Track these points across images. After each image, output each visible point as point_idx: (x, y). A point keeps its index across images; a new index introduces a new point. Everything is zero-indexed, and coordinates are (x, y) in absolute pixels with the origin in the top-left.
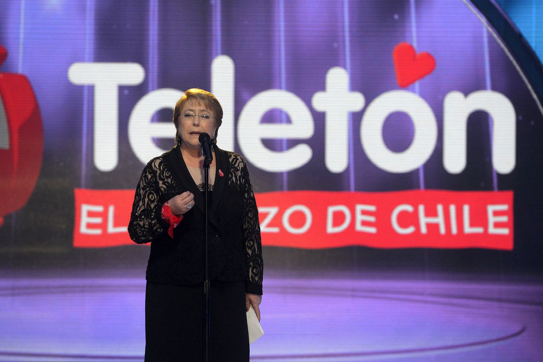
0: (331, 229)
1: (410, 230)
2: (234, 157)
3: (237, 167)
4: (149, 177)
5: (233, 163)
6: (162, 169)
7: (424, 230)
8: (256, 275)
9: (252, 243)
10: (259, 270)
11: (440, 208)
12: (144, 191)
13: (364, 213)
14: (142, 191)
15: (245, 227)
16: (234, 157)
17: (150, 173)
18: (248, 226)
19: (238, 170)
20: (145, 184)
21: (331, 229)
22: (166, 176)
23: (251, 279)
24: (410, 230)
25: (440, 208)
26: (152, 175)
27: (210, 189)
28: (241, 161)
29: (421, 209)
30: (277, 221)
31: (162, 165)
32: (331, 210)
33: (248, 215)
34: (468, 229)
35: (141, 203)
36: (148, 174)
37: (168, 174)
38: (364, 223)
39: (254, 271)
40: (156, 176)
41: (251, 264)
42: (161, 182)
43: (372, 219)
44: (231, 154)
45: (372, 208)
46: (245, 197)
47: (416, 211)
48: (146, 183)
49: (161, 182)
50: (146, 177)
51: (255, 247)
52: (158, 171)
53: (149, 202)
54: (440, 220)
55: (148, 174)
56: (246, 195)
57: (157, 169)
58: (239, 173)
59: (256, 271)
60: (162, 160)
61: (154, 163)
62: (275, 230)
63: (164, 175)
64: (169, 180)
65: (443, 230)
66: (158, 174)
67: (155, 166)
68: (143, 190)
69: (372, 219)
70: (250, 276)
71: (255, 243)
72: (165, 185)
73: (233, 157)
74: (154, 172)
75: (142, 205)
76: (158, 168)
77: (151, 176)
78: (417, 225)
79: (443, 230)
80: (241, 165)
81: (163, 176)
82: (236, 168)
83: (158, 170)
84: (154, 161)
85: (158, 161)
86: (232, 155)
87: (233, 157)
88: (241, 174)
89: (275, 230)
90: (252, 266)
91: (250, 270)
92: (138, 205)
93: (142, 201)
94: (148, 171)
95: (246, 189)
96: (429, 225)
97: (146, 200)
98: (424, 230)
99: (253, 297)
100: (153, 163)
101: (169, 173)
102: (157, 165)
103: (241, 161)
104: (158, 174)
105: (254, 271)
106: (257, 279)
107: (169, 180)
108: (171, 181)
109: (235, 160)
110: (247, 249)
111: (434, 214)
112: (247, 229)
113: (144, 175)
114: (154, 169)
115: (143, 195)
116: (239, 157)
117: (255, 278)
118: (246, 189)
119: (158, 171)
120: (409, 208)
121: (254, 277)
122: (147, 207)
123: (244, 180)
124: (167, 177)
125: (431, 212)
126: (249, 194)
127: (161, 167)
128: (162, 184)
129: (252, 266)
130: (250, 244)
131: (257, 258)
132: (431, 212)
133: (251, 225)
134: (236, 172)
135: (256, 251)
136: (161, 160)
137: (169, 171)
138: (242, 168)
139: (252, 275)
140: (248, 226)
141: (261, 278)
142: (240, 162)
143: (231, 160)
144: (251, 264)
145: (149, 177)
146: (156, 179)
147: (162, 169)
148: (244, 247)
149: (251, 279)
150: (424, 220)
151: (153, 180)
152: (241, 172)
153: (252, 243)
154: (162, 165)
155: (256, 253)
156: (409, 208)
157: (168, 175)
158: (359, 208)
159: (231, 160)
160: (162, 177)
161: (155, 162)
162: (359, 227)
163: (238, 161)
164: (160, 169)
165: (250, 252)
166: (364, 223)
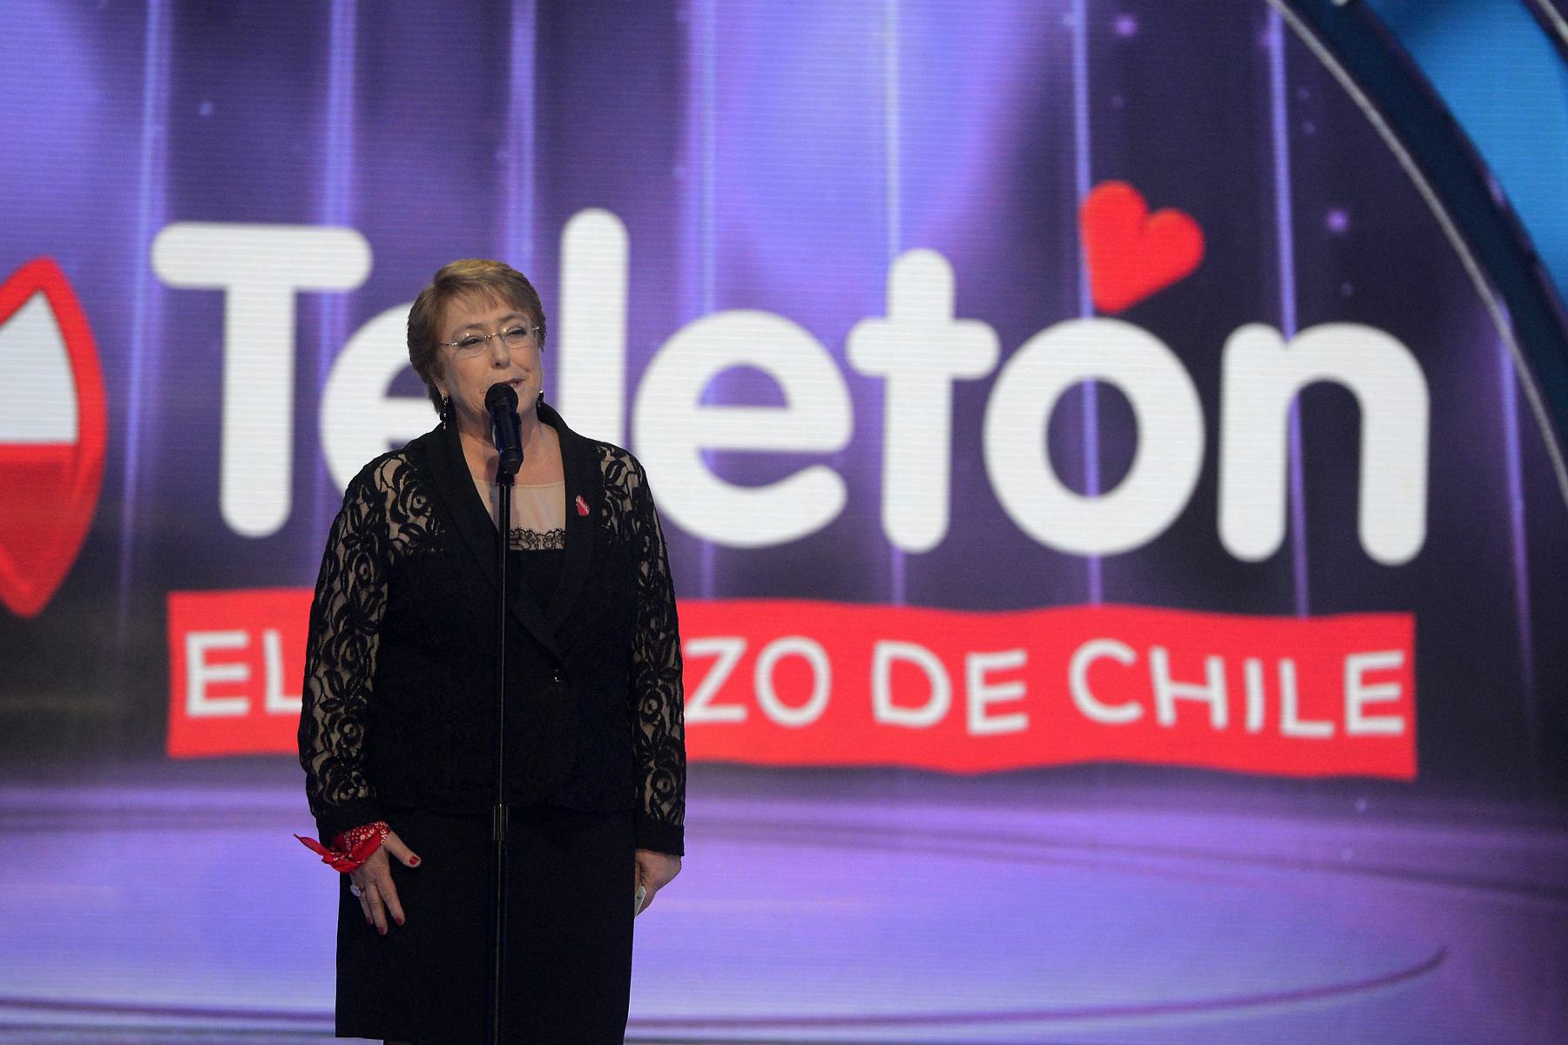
2: (613, 459)
3: (623, 486)
4: (365, 509)
5: (611, 477)
6: (402, 487)
8: (665, 797)
9: (654, 704)
10: (675, 784)
12: (348, 552)
14: (341, 550)
15: (637, 658)
16: (613, 459)
17: (366, 499)
18: (648, 656)
19: (624, 497)
20: (351, 530)
22: (412, 509)
23: (648, 810)
25: (1215, 668)
26: (371, 505)
27: (537, 546)
28: (633, 470)
29: (1159, 660)
30: (739, 687)
31: (404, 476)
33: (649, 625)
34: (1291, 725)
35: (337, 585)
36: (360, 500)
37: (419, 501)
38: (993, 710)
39: (660, 785)
40: (384, 509)
41: (652, 764)
42: (395, 527)
43: (1014, 691)
44: (605, 449)
45: (1014, 659)
46: (643, 574)
47: (1143, 666)
48: (353, 529)
49: (395, 527)
50: (356, 507)
51: (663, 717)
52: (391, 495)
53: (357, 584)
54: (1215, 693)
55: (360, 500)
56: (645, 568)
57: (388, 487)
58: (628, 506)
59: (665, 785)
60: (405, 460)
61: (381, 472)
63: (408, 506)
64: (422, 522)
65: (1219, 717)
66: (388, 505)
67: (382, 478)
68: (347, 547)
69: (1014, 691)
70: (648, 799)
71: (664, 707)
72: (408, 533)
73: (609, 458)
74: (377, 498)
75: (339, 592)
76: (391, 483)
77: (369, 507)
79: (1219, 717)
80: (633, 482)
81: (405, 510)
82: (619, 489)
83: (390, 490)
84: (382, 465)
85: (394, 464)
86: (608, 453)
87: (609, 458)
88: (633, 507)
90: (653, 772)
91: (648, 785)
92: (330, 590)
93: (341, 576)
94: (361, 493)
95: (645, 550)
97: (352, 577)
99: (651, 861)
100: (379, 469)
101: (423, 500)
102: (389, 477)
103: (633, 470)
104: (388, 505)
105: (660, 785)
106: (666, 808)
107: (422, 522)
108: (428, 525)
109: (615, 467)
110: (641, 723)
112: (642, 664)
113: (351, 501)
114: (379, 488)
115: (344, 561)
116: (626, 460)
117: (662, 807)
118: (645, 550)
119: (391, 495)
120: (1122, 653)
121: (658, 802)
122: (352, 600)
123: (638, 524)
124: (417, 513)
126: (653, 565)
127: (401, 481)
128: (400, 531)
129: (653, 772)
130: (650, 707)
131: (668, 748)
132: (1188, 670)
133: (653, 650)
134: (619, 502)
135: (667, 730)
136: (400, 463)
137: (423, 494)
138: (634, 489)
139: (653, 796)
140: (648, 656)
141: (679, 807)
142: (629, 473)
143: (604, 466)
144: (652, 764)
145: (365, 509)
146: (383, 517)
147: (402, 487)
148: (634, 715)
149: (648, 810)
150: (1167, 692)
151: (374, 519)
152: (633, 502)
153: (654, 704)
154: (404, 476)
155: (667, 733)
156: (1122, 653)
157: (419, 506)
158: (978, 664)
159: (604, 466)
160: (401, 510)
161: (382, 469)
162: (979, 724)
163: (624, 471)
164: (396, 489)
165: (648, 730)
166: (993, 710)
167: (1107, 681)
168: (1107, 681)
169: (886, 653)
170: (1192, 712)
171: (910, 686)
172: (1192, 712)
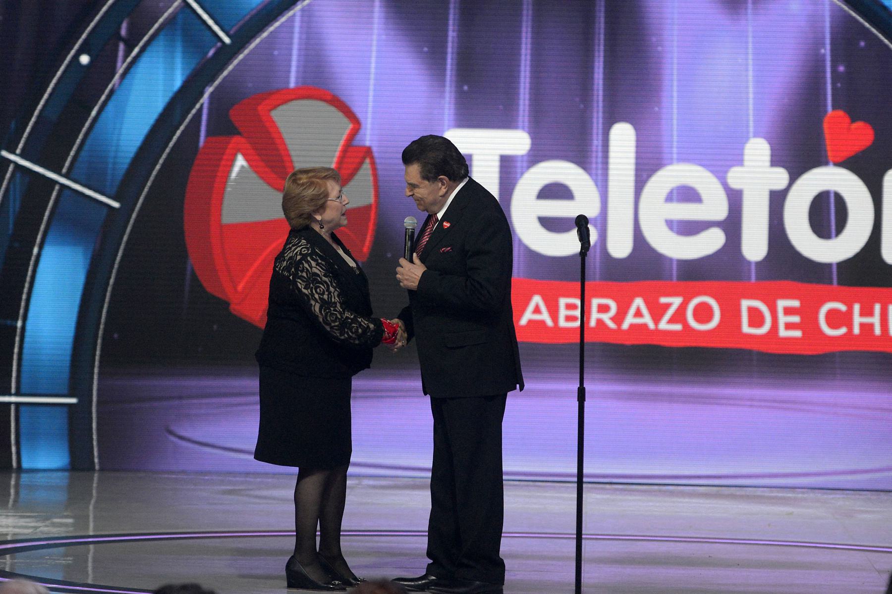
0: (746, 329)
1: (843, 331)
7: (856, 330)
11: (877, 308)
13: (788, 311)
21: (746, 329)
24: (843, 331)
25: (877, 308)
29: (857, 308)
32: (745, 304)
45: (796, 303)
47: (850, 312)
54: (876, 320)
62: (678, 327)
69: (796, 319)
78: (850, 326)
89: (678, 327)
96: (862, 325)
98: (856, 330)
111: (871, 314)
120: (843, 307)
125: (867, 311)
132: (867, 311)
156: (843, 307)
158: (782, 304)
167: (834, 319)
168: (834, 319)
169: (745, 304)
170: (867, 328)
171: (756, 318)
172: (867, 328)
